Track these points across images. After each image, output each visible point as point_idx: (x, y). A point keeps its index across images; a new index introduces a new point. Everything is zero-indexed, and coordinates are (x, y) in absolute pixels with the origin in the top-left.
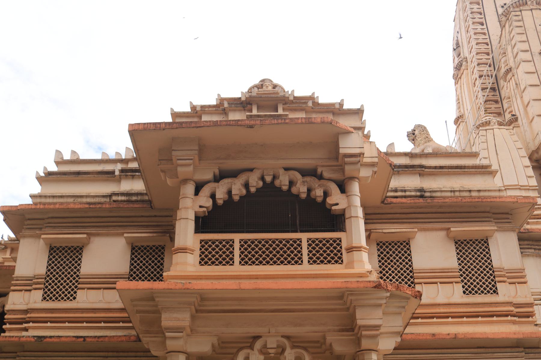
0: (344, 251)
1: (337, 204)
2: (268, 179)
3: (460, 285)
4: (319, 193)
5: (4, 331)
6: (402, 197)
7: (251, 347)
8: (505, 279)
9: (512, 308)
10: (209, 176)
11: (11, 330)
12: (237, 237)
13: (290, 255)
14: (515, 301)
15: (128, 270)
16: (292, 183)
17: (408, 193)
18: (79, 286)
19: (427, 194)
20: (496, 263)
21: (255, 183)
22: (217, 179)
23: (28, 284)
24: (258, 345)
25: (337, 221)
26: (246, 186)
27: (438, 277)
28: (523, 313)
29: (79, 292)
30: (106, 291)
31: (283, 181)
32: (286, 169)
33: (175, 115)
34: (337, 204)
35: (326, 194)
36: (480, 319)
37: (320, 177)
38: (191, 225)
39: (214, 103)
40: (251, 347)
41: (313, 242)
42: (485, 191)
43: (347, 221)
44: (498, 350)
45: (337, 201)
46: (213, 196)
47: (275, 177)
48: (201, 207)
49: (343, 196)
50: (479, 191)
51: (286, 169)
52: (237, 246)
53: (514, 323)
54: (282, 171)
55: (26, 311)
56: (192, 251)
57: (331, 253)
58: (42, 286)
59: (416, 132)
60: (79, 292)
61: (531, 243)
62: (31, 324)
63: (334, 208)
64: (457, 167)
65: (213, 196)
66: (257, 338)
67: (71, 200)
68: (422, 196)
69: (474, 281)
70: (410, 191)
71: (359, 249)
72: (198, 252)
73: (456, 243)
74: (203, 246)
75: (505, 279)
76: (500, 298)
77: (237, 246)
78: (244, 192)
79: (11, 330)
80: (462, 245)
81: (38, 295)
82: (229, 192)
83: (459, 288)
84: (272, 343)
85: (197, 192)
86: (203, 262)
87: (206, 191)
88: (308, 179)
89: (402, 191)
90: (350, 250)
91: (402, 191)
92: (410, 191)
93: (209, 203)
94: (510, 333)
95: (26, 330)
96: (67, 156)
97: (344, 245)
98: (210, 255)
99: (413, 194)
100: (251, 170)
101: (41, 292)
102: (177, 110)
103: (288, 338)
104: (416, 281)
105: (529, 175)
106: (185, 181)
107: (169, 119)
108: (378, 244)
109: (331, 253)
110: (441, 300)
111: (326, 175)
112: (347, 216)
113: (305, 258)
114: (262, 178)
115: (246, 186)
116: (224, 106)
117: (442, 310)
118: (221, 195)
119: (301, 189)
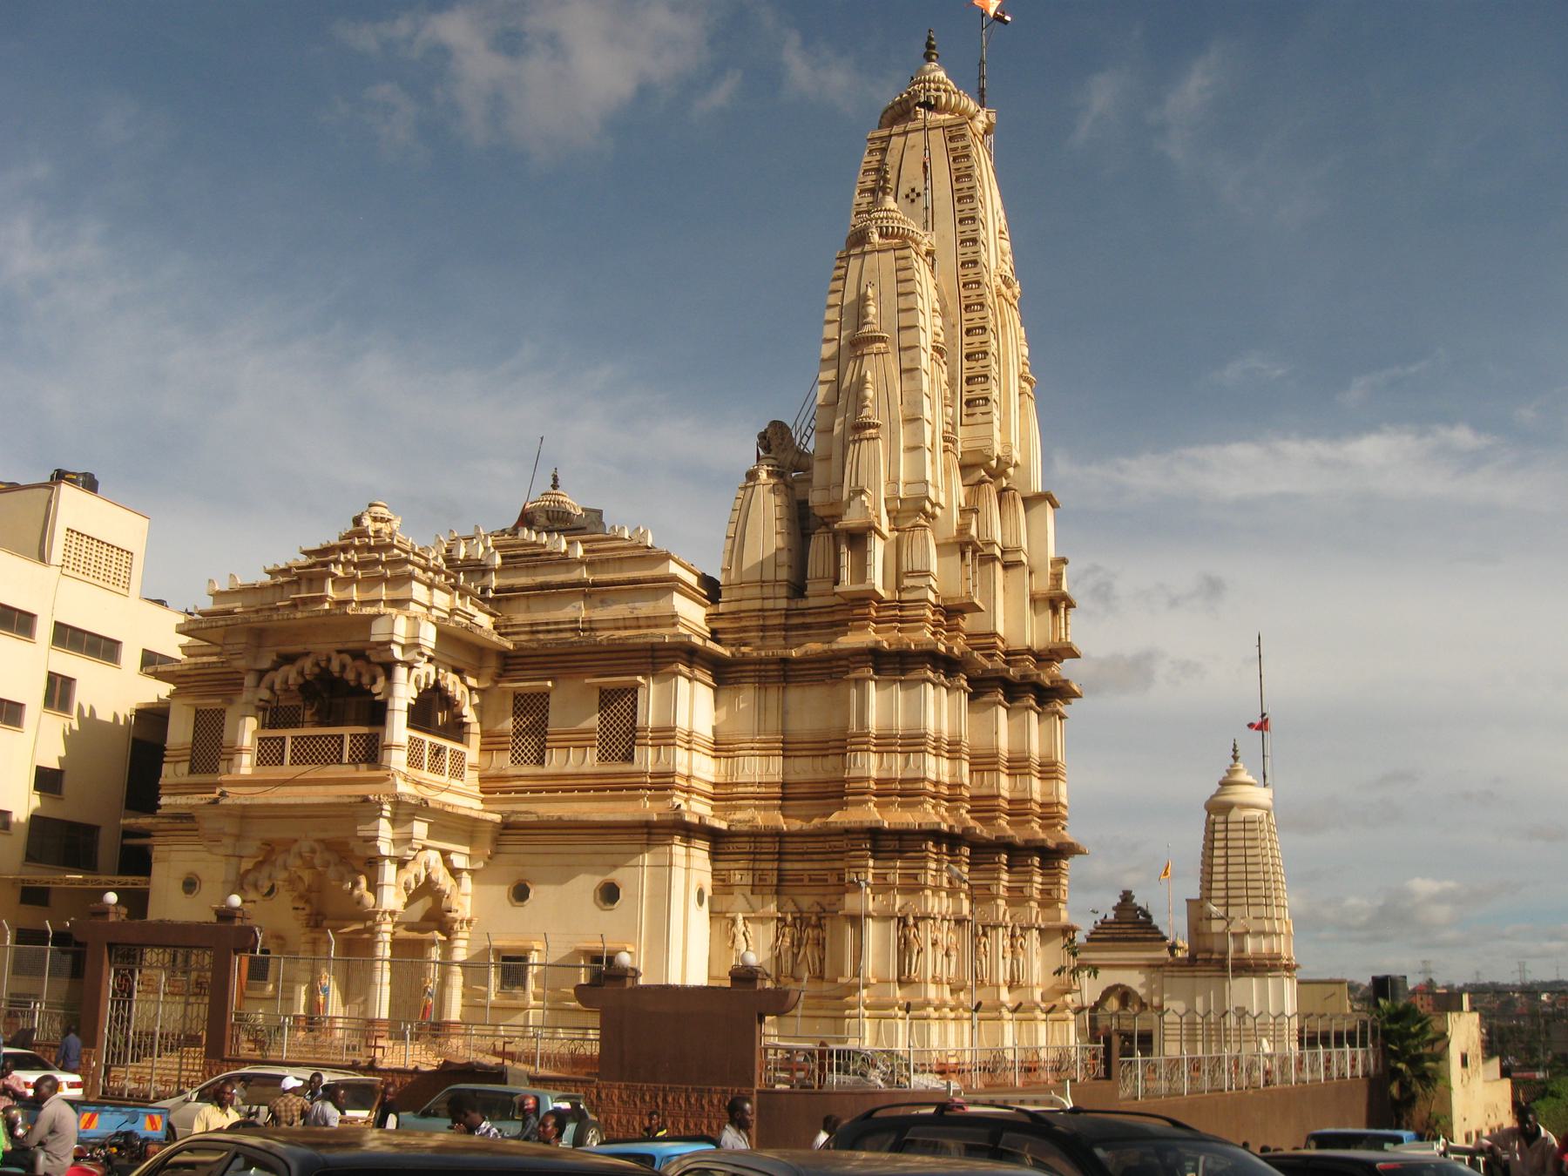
2: (323, 664)
16: (343, 667)
22: (275, 667)
24: (295, 848)
25: (378, 713)
26: (301, 673)
31: (335, 667)
32: (339, 652)
35: (374, 681)
40: (288, 851)
43: (389, 715)
47: (329, 660)
52: (289, 742)
54: (334, 655)
77: (289, 742)
80: (607, 698)
83: (592, 756)
86: (262, 760)
87: (267, 679)
98: (269, 753)
100: (307, 654)
113: (346, 758)
114: (317, 664)
119: (350, 676)
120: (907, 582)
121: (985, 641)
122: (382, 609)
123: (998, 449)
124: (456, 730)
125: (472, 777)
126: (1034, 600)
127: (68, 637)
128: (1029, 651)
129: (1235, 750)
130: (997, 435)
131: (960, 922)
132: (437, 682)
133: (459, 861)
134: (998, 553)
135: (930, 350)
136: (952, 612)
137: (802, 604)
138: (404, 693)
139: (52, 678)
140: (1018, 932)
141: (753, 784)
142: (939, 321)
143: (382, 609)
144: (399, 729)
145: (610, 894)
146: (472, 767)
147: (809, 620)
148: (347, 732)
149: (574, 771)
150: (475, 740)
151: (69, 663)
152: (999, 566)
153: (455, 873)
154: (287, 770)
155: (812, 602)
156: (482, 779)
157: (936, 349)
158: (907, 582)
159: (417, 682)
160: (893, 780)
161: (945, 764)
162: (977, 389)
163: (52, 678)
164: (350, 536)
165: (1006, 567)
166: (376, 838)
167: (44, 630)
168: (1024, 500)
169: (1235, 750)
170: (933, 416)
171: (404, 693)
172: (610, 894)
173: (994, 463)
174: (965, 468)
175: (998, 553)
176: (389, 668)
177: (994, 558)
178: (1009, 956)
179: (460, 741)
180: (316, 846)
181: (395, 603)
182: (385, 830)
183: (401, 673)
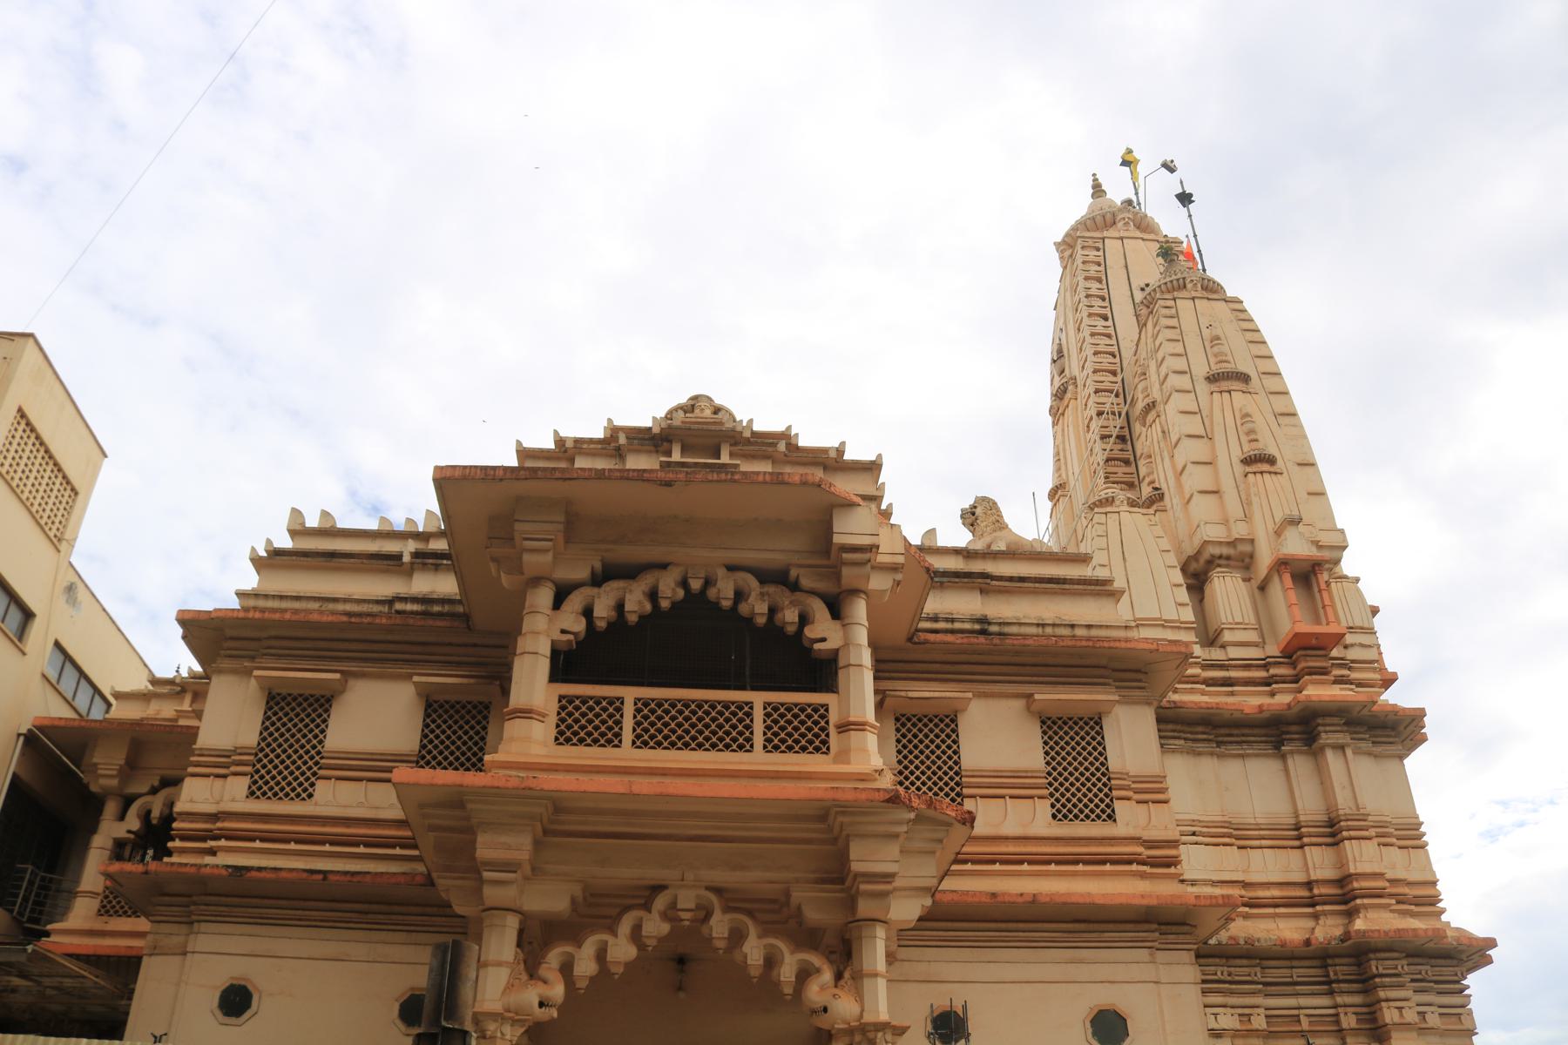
0: (832, 730)
1: (823, 640)
2: (696, 585)
3: (1048, 803)
4: (790, 616)
5: (169, 853)
6: (946, 631)
7: (647, 907)
8: (1130, 794)
9: (1140, 849)
10: (582, 573)
11: (183, 851)
12: (629, 694)
13: (730, 732)
14: (1146, 835)
15: (417, 748)
16: (739, 596)
17: (957, 625)
18: (321, 772)
19: (994, 629)
20: (1114, 764)
21: (669, 590)
22: (598, 580)
23: (223, 764)
24: (660, 902)
25: (821, 672)
26: (653, 595)
27: (1007, 785)
28: (1159, 857)
29: (320, 784)
30: (371, 785)
31: (724, 591)
32: (731, 568)
33: (523, 453)
34: (823, 640)
35: (804, 620)
36: (1080, 867)
37: (795, 587)
38: (544, 666)
39: (599, 434)
40: (647, 907)
41: (776, 709)
42: (1101, 627)
44: (1111, 926)
45: (824, 632)
46: (588, 613)
47: (708, 583)
48: (563, 632)
49: (836, 625)
50: (1089, 627)
51: (731, 568)
52: (629, 710)
53: (1143, 876)
54: (721, 572)
55: (215, 817)
56: (542, 716)
57: (807, 733)
58: (249, 769)
59: (978, 511)
60: (320, 784)
61: (1179, 727)
62: (223, 842)
63: (817, 646)
64: (1051, 580)
65: (588, 613)
66: (658, 889)
67: (315, 605)
68: (983, 632)
69: (1074, 795)
70: (962, 621)
71: (861, 726)
72: (553, 719)
73: (1043, 722)
74: (563, 708)
75: (1130, 794)
76: (1119, 829)
77: (629, 710)
78: (648, 607)
79: (183, 851)
80: (1053, 726)
81: (240, 785)
82: (620, 607)
83: (1044, 808)
84: (687, 900)
85: (558, 604)
87: (575, 602)
88: (771, 589)
89: (947, 620)
90: (845, 727)
91: (947, 620)
92: (962, 621)
93: (580, 626)
94: (1134, 896)
95: (212, 852)
96: (312, 521)
97: (833, 717)
98: (575, 726)
99: (967, 626)
100: (664, 566)
101: (246, 781)
102: (526, 444)
103: (718, 891)
104: (965, 791)
105: (1180, 600)
106: (536, 581)
107: (512, 461)
108: (897, 719)
110: (1010, 829)
111: (806, 582)
112: (841, 663)
113: (759, 740)
114: (684, 583)
115: (653, 595)
116: (619, 441)
117: (1011, 848)
118: (603, 611)
119: (757, 607)
137: (1216, 654)
147: (1233, 674)
149: (1019, 832)
155: (1234, 652)
180: (713, 897)
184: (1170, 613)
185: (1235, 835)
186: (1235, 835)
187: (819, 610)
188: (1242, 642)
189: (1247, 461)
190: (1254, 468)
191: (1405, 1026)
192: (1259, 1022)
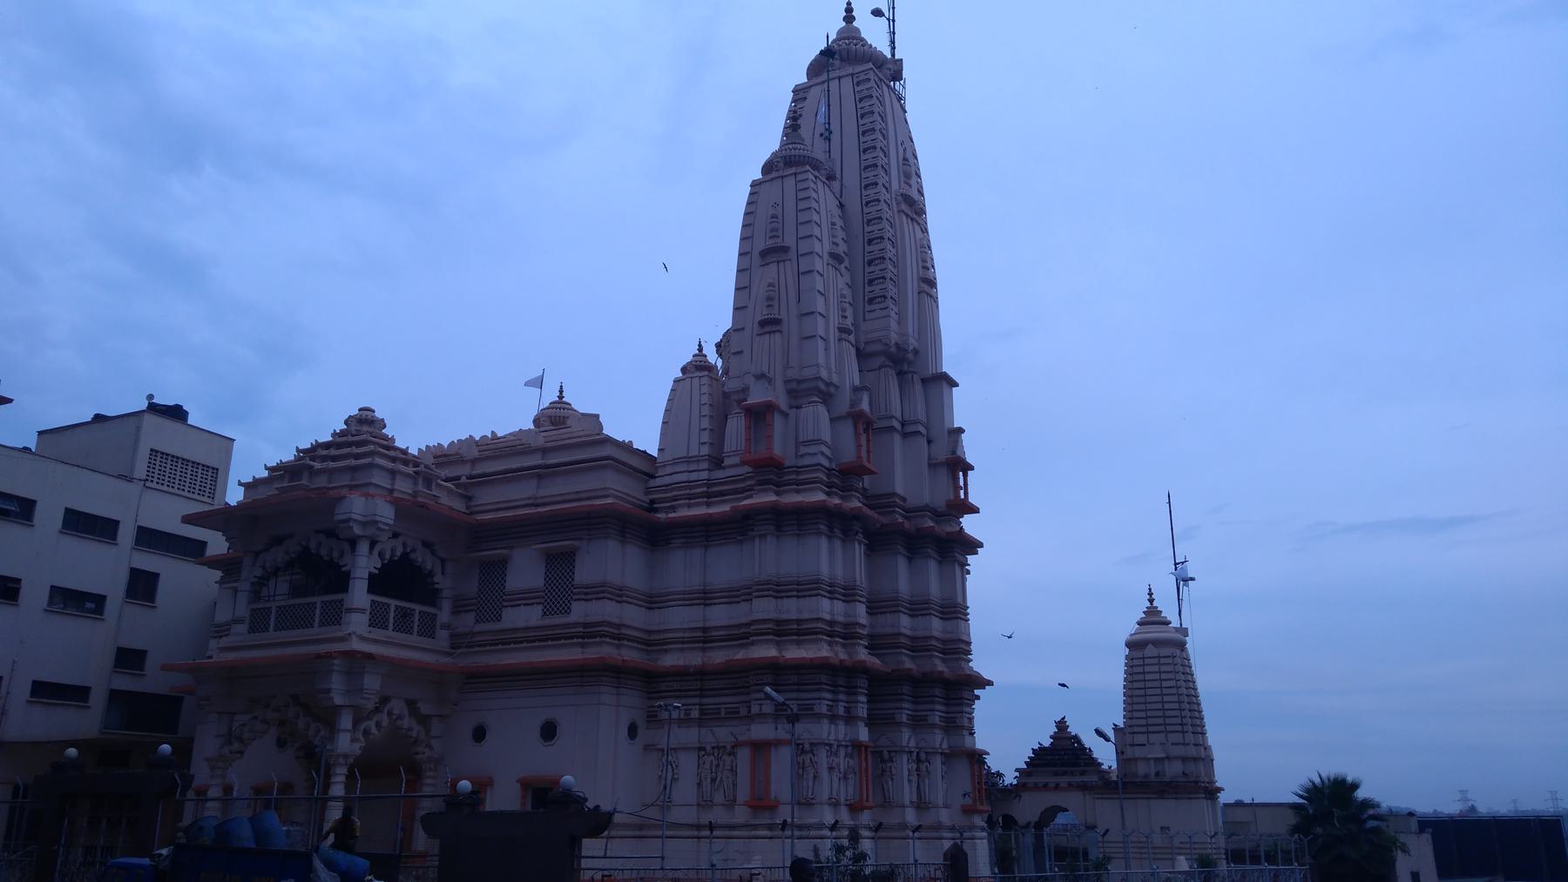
3: (540, 607)
4: (335, 555)
25: (341, 582)
27: (525, 597)
31: (313, 545)
32: (318, 532)
35: (342, 555)
46: (263, 568)
76: (572, 618)
90: (350, 610)
102: (270, 465)
107: (265, 474)
109: (335, 615)
110: (521, 624)
119: (324, 552)
120: (803, 450)
121: (882, 501)
122: (344, 492)
123: (894, 338)
124: (431, 596)
125: (443, 634)
126: (933, 465)
127: (148, 538)
128: (926, 508)
129: (1150, 594)
130: (894, 325)
131: (857, 746)
132: (405, 555)
133: (425, 709)
134: (897, 425)
135: (826, 256)
136: (846, 476)
137: (720, 474)
138: (364, 565)
139: (135, 574)
140: (923, 756)
141: (684, 630)
142: (841, 234)
143: (344, 492)
144: (359, 595)
145: (549, 731)
146: (444, 627)
148: (318, 600)
150: (446, 606)
151: (148, 561)
152: (897, 438)
153: (424, 720)
154: (272, 635)
156: (452, 636)
157: (834, 256)
158: (803, 450)
159: (380, 554)
160: (789, 621)
161: (839, 606)
162: (877, 288)
163: (135, 574)
164: (343, 433)
165: (905, 435)
166: (329, 691)
167: (126, 534)
168: (924, 381)
169: (1150, 594)
170: (827, 310)
171: (364, 565)
172: (549, 731)
173: (893, 349)
174: (860, 354)
175: (897, 425)
176: (353, 542)
177: (892, 429)
178: (915, 779)
179: (433, 605)
181: (352, 488)
182: (337, 683)
183: (363, 547)
184: (694, 452)
185: (705, 597)
186: (705, 597)
187: (347, 547)
188: (733, 468)
189: (763, 323)
190: (767, 329)
191: (764, 716)
192: (695, 714)
